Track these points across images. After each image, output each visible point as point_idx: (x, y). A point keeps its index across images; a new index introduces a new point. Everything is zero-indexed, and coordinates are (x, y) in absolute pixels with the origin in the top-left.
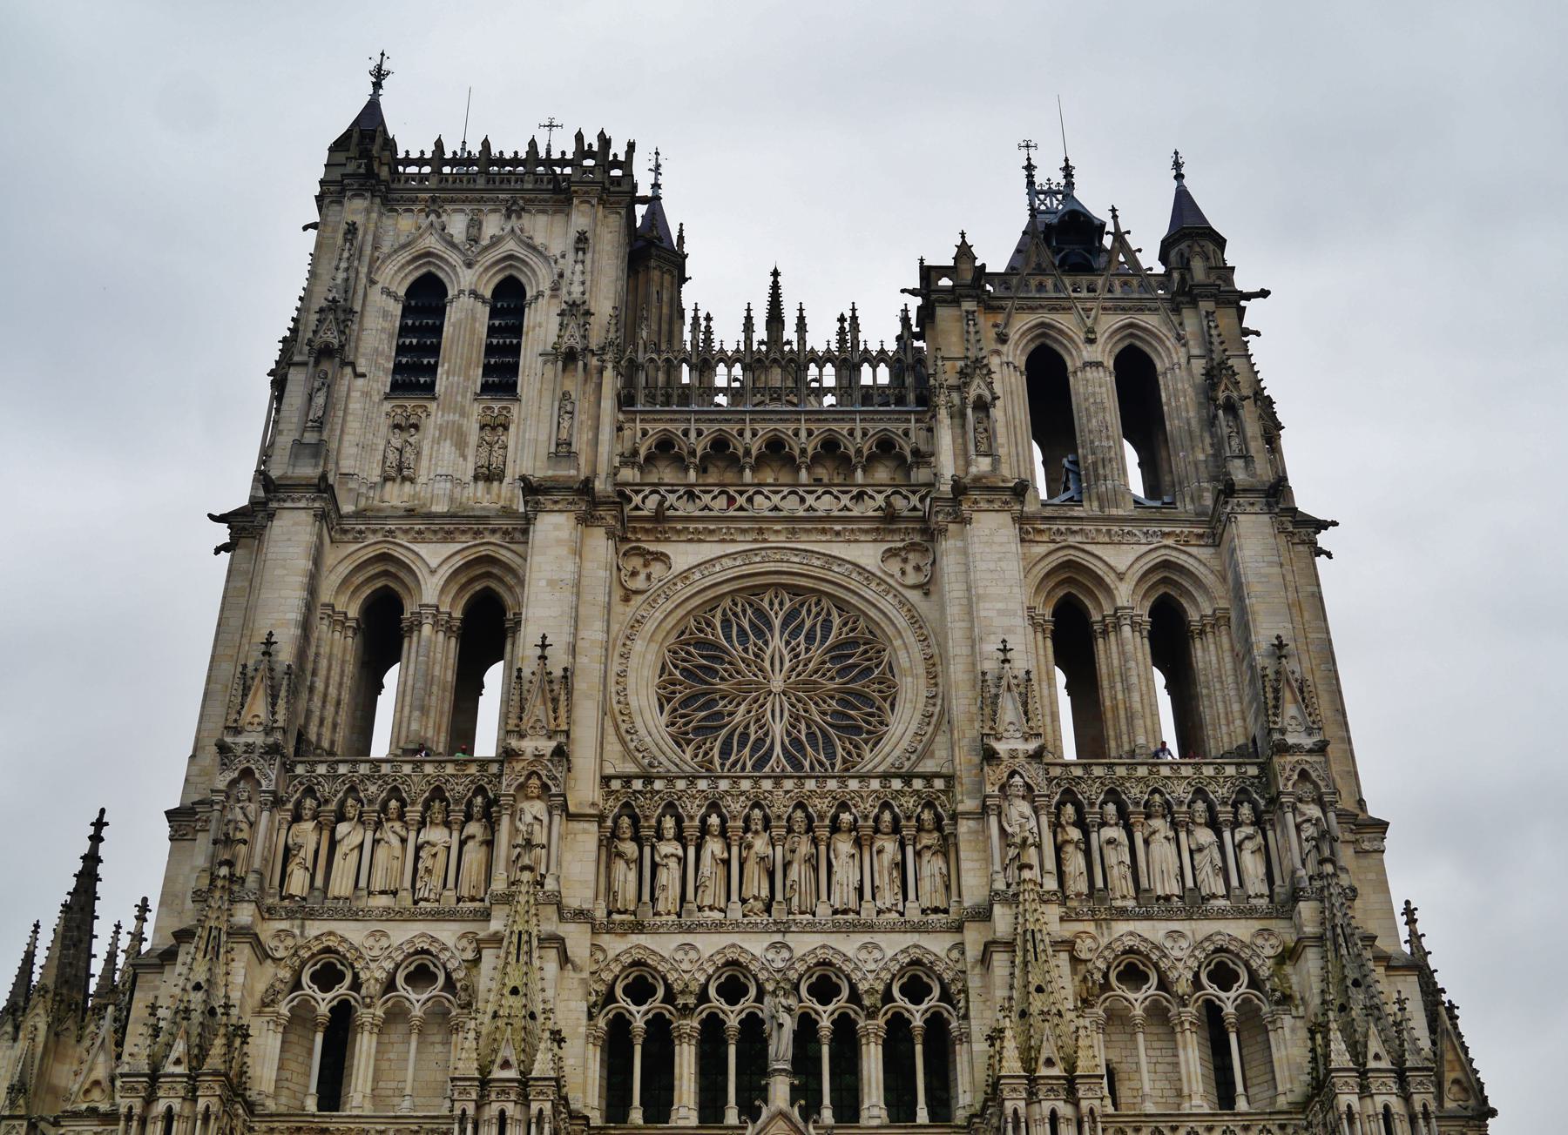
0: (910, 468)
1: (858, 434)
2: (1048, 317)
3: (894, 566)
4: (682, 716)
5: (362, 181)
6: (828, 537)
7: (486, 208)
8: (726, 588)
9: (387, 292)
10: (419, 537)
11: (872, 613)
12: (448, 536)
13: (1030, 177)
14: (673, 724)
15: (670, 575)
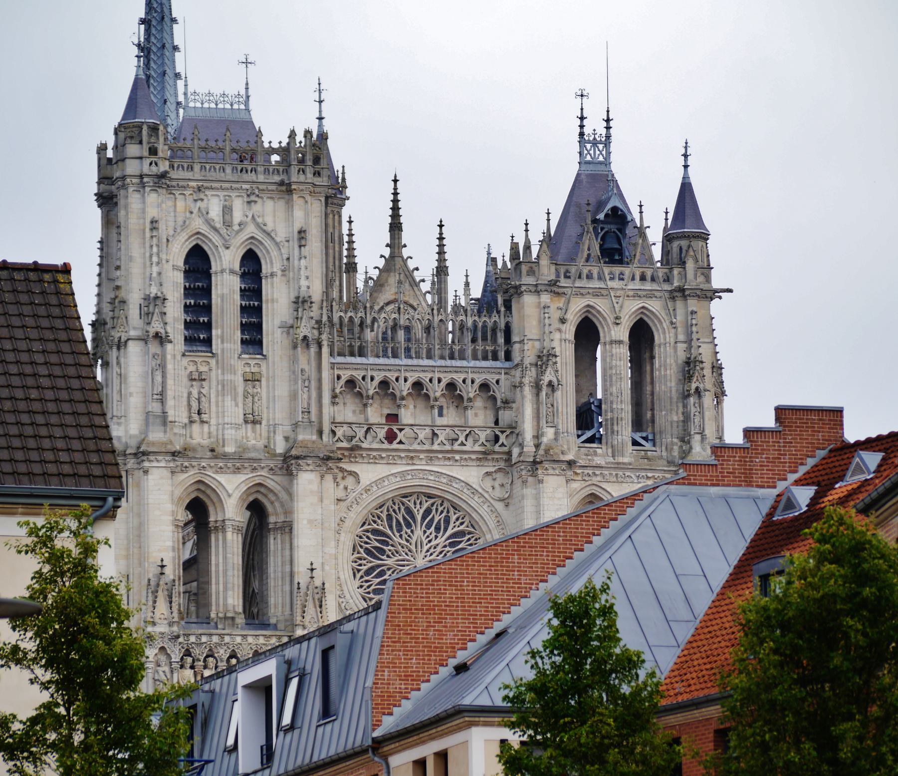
0: (499, 408)
1: (469, 382)
2: (592, 301)
3: (488, 483)
4: (367, 581)
5: (156, 180)
6: (451, 463)
7: (233, 194)
8: (390, 495)
9: (175, 268)
10: (220, 470)
11: (474, 515)
12: (237, 470)
13: (582, 126)
14: (361, 587)
15: (360, 488)
